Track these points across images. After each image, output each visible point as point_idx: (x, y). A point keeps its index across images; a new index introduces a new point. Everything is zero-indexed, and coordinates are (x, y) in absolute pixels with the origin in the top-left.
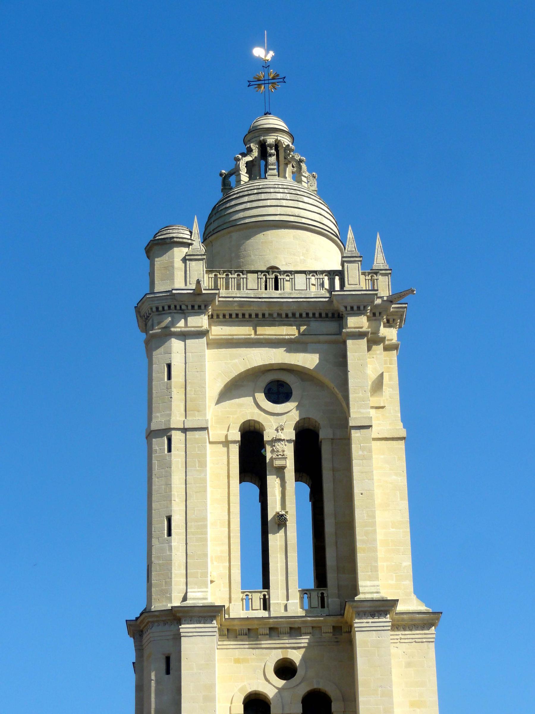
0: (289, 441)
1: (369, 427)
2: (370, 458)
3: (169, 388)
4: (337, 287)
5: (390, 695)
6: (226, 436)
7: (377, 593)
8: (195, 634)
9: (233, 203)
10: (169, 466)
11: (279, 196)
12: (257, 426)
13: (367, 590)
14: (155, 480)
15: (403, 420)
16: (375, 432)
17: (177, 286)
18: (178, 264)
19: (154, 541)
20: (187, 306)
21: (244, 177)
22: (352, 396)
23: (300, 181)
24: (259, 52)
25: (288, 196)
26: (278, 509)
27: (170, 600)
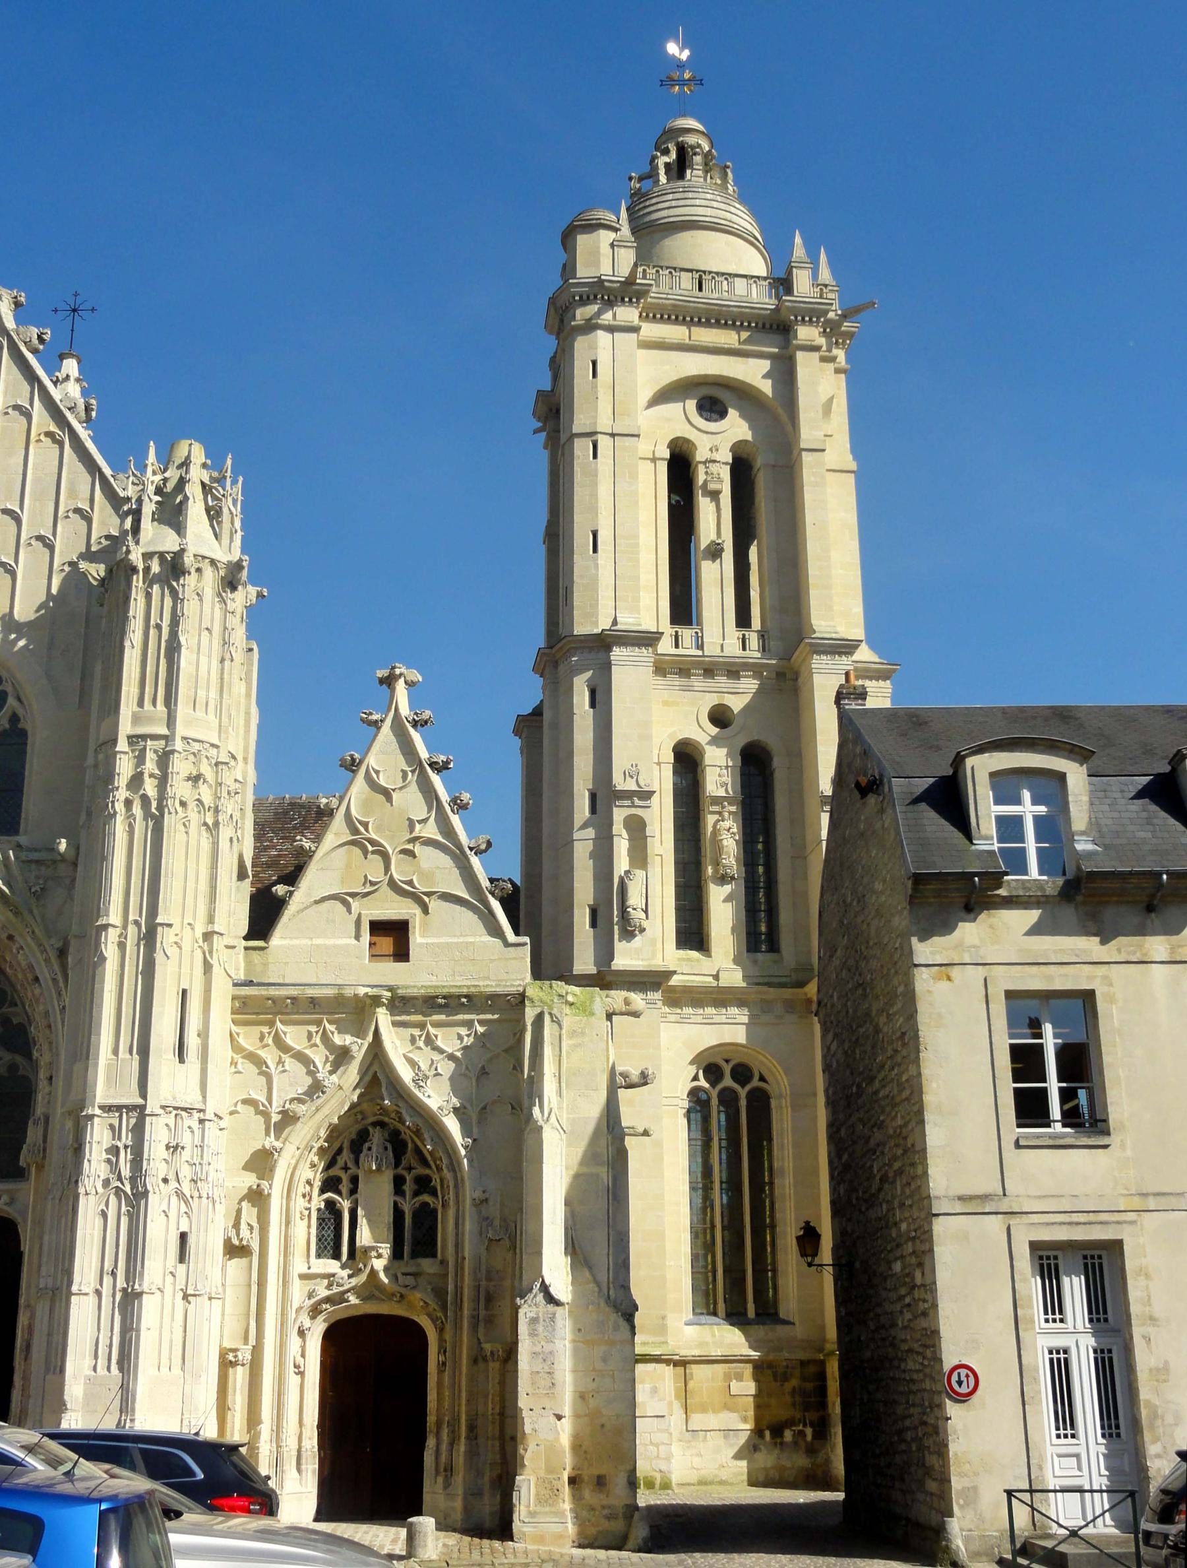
0: (726, 464)
1: (823, 450)
6: (654, 452)
7: (836, 633)
8: (628, 663)
9: (654, 201)
10: (595, 474)
11: (709, 196)
12: (685, 447)
13: (822, 629)
15: (852, 452)
20: (616, 298)
21: (663, 179)
24: (672, 48)
25: (719, 198)
26: (713, 536)
27: (596, 624)
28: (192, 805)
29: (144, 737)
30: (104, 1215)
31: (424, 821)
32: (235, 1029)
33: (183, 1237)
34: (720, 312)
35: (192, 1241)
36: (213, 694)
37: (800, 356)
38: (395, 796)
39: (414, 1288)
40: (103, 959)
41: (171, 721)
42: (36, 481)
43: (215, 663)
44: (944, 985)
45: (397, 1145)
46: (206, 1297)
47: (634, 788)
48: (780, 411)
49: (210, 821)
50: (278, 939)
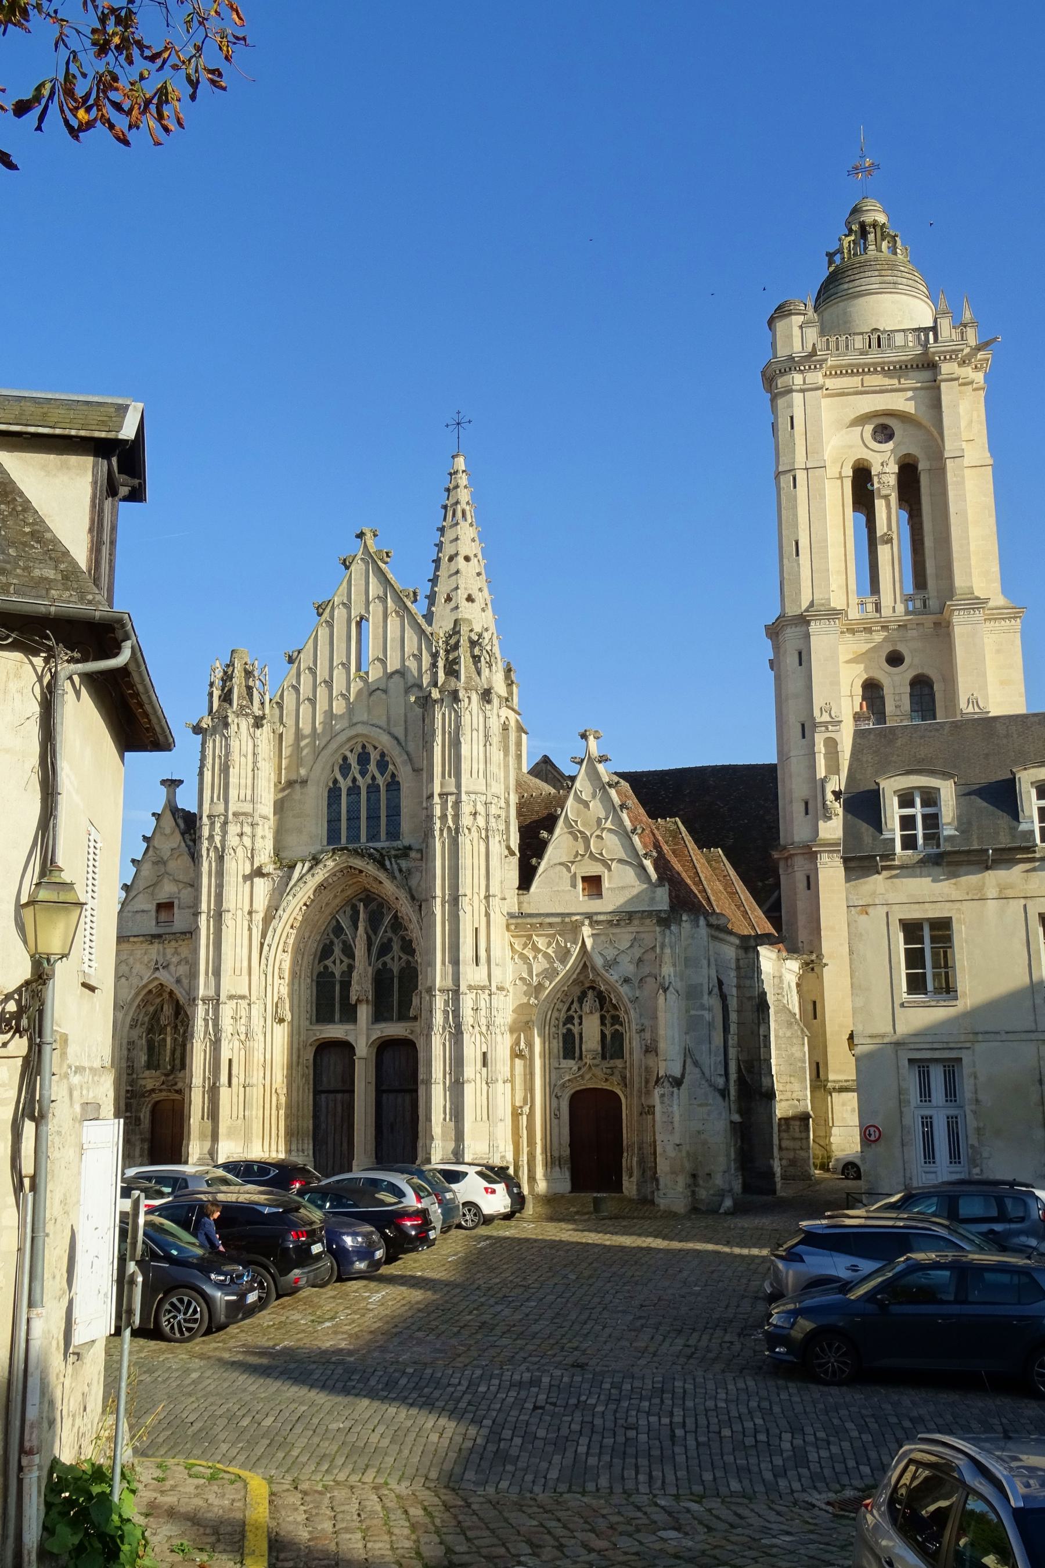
2: (963, 483)
3: (792, 436)
4: (931, 340)
5: (984, 675)
6: (840, 473)
10: (795, 499)
14: (784, 512)
15: (990, 451)
16: (966, 462)
17: (795, 350)
18: (796, 331)
19: (785, 561)
22: (946, 432)
23: (895, 254)
28: (474, 829)
29: (447, 794)
30: (444, 1045)
31: (606, 819)
32: (512, 940)
33: (485, 1054)
34: (884, 363)
35: (489, 1056)
36: (482, 767)
37: (943, 385)
38: (591, 805)
39: (612, 1075)
40: (433, 914)
41: (458, 786)
42: (392, 640)
43: (482, 748)
44: (864, 917)
45: (602, 998)
46: (500, 1082)
47: (828, 719)
48: (932, 429)
49: (483, 836)
50: (533, 889)
